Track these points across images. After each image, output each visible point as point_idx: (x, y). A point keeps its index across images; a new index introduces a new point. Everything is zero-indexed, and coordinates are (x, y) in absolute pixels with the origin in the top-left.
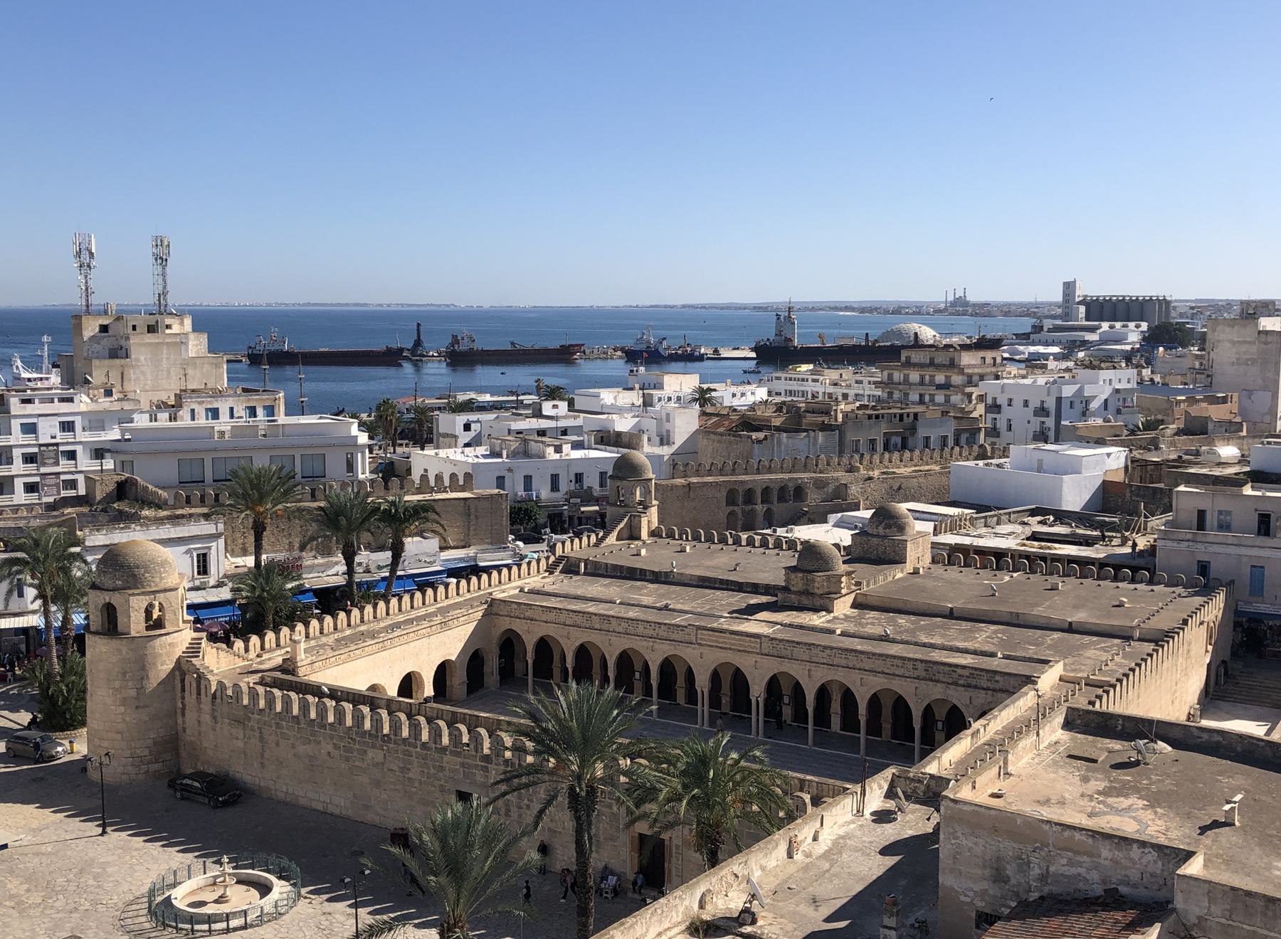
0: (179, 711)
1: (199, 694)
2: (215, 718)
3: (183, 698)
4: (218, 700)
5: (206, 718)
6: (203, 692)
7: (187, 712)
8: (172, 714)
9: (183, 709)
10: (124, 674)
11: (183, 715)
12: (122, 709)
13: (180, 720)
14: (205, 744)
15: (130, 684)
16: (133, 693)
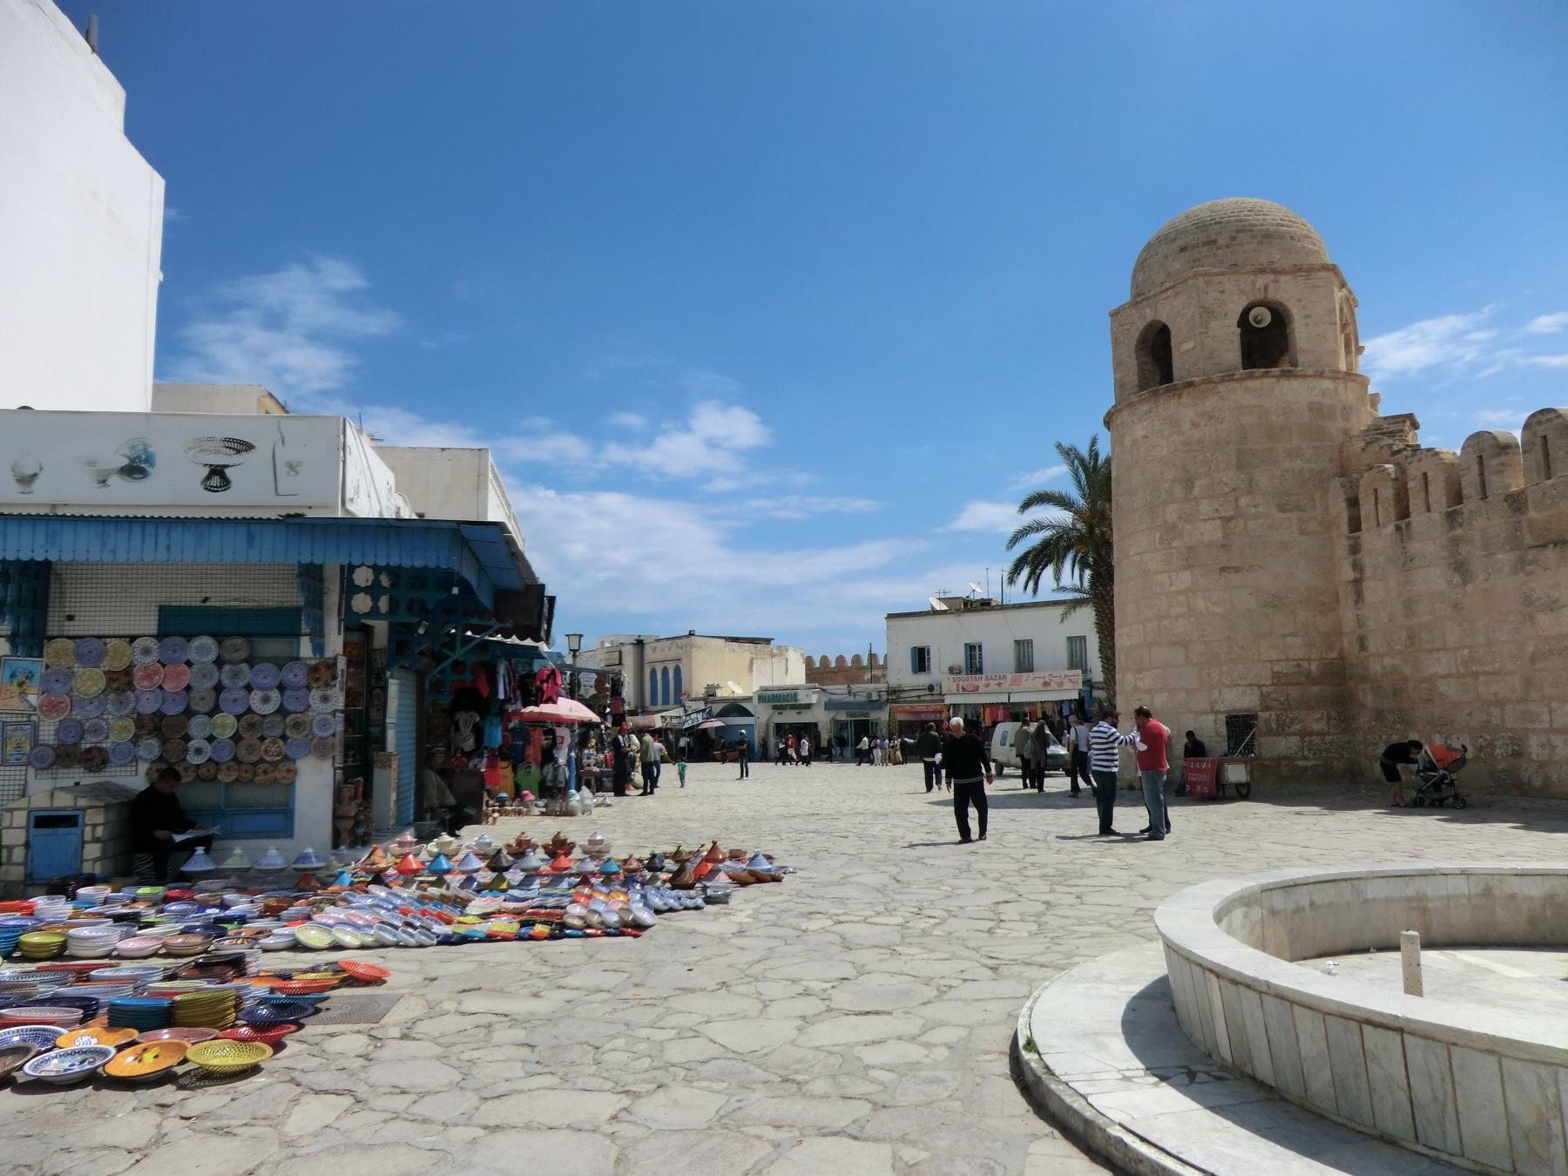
0: (1347, 594)
1: (1404, 513)
2: (1460, 567)
3: (1355, 549)
4: (1471, 503)
5: (1433, 578)
6: (1415, 504)
7: (1368, 586)
8: (1326, 602)
9: (1357, 582)
10: (1188, 483)
11: (1359, 596)
12: (1185, 578)
13: (1348, 616)
14: (1438, 665)
15: (1205, 508)
16: (1211, 531)
